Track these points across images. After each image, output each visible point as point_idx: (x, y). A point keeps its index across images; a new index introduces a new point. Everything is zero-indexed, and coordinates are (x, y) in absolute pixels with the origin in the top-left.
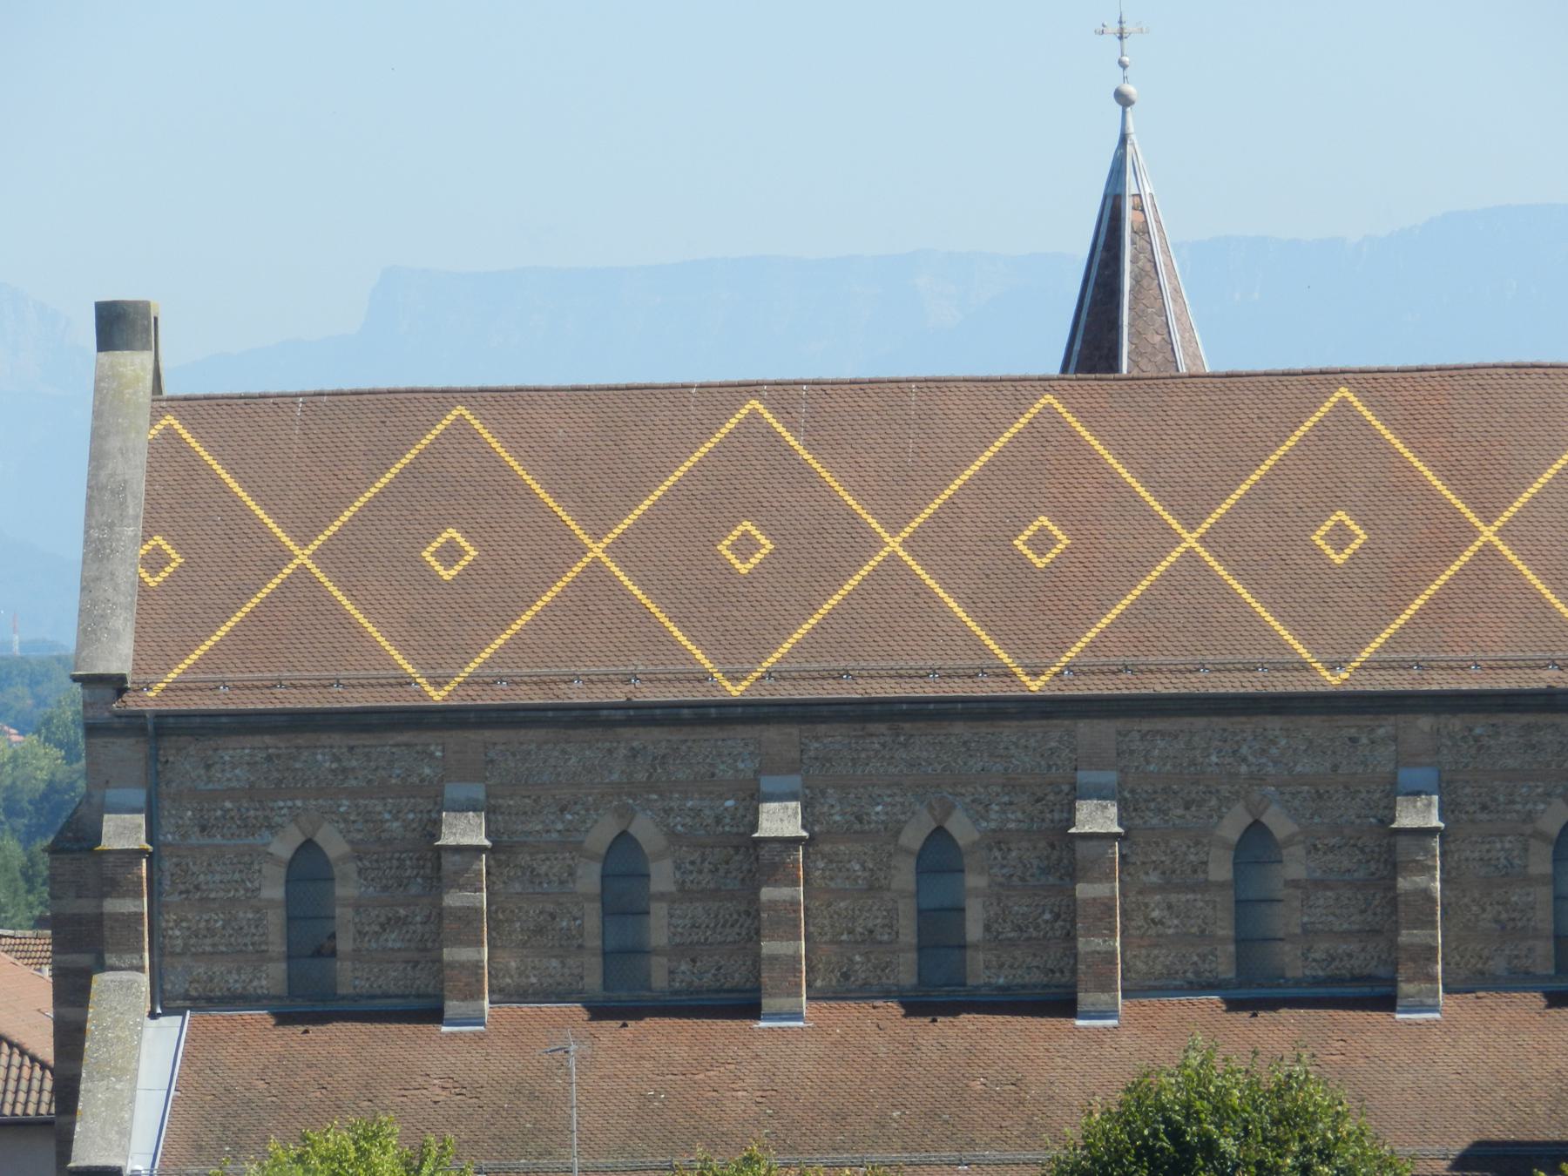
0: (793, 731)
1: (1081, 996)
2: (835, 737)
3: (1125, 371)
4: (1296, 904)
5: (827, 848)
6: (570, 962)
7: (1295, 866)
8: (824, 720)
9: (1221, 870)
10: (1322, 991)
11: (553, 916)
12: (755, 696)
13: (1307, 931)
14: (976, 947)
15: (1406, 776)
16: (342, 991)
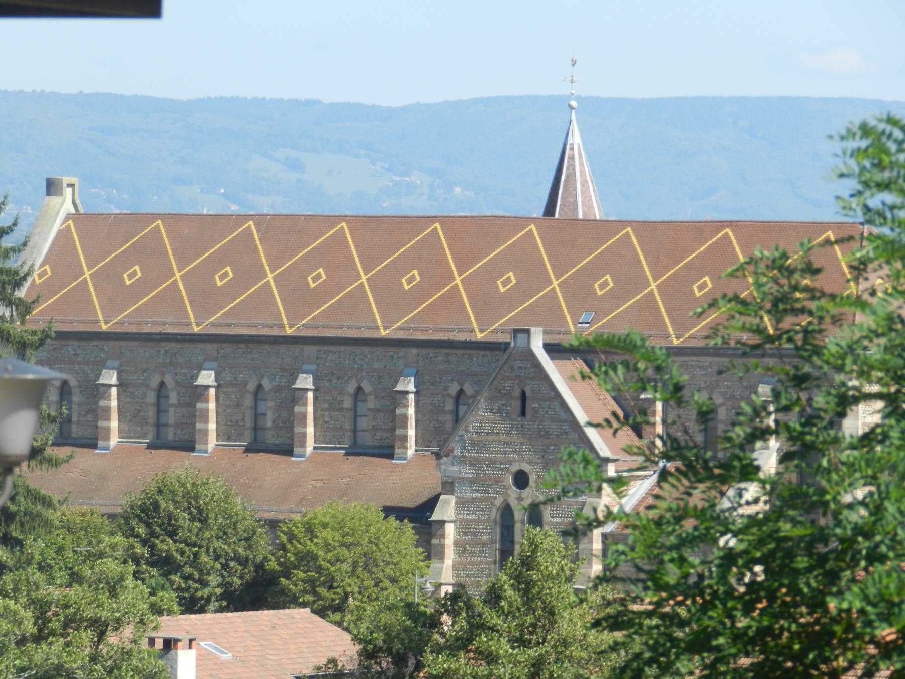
0: (215, 345)
1: (295, 449)
2: (228, 348)
3: (557, 216)
4: (371, 418)
5: (224, 390)
6: (145, 428)
7: (371, 403)
8: (225, 342)
9: (348, 403)
10: (376, 451)
11: (139, 411)
12: (685, 345)
13: (374, 428)
14: (269, 429)
15: (407, 370)
16: (268, 441)
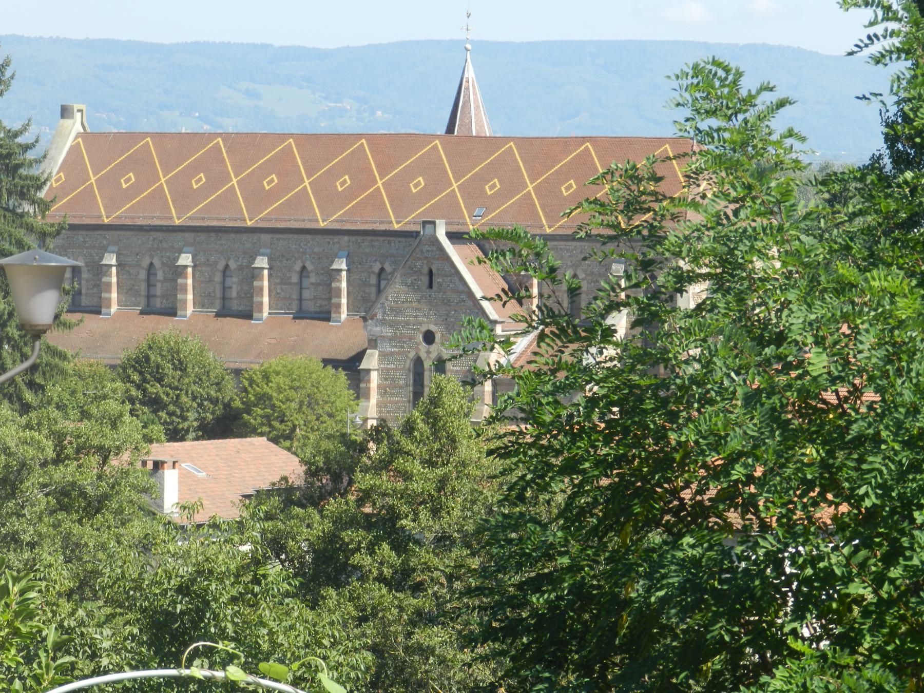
0: (192, 235)
2: (202, 237)
7: (313, 279)
9: (295, 279)
13: (315, 297)
